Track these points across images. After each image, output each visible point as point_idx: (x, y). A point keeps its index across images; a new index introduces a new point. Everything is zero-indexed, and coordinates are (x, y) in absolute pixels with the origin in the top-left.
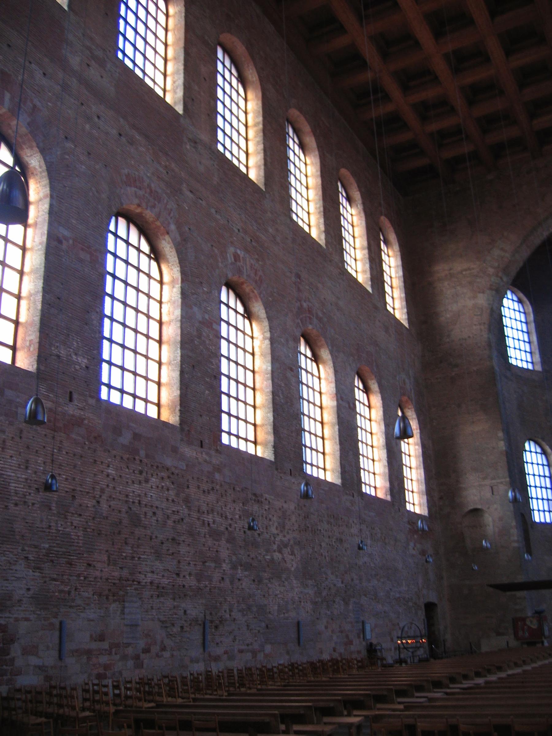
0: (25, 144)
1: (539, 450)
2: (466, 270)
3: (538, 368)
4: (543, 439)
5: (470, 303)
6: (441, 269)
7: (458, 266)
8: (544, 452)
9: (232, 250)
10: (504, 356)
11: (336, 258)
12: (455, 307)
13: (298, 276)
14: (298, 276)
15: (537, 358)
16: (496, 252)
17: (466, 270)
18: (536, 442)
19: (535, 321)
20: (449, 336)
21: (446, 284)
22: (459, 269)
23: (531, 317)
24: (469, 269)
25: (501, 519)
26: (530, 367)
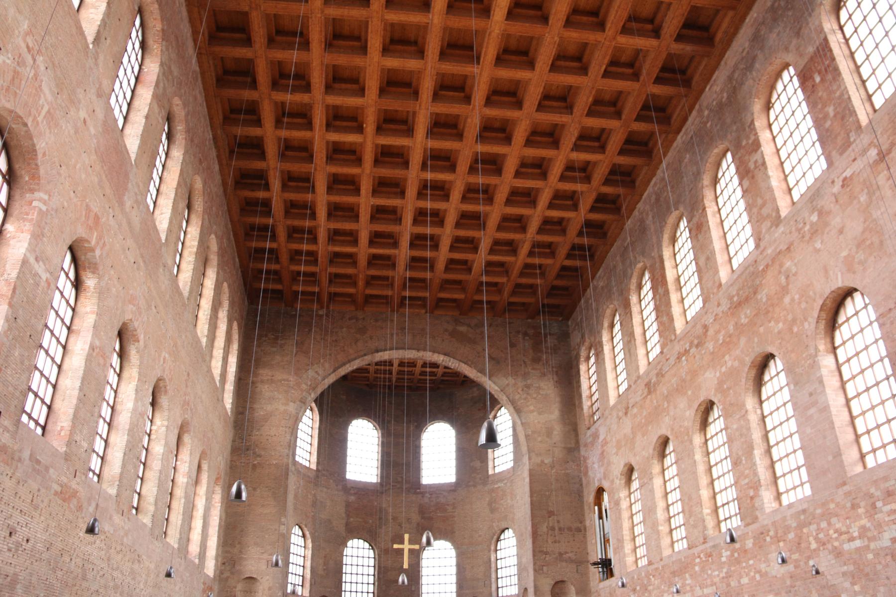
0: (89, 268)
1: (301, 534)
2: (284, 380)
3: (314, 467)
4: (306, 526)
5: (282, 408)
6: (265, 373)
7: (279, 375)
8: (304, 536)
9: (164, 354)
10: (294, 454)
11: (208, 358)
12: (269, 408)
13: (188, 374)
14: (188, 374)
15: (314, 458)
16: (311, 373)
17: (284, 380)
18: (300, 527)
19: (319, 428)
20: (259, 430)
21: (266, 386)
22: (280, 378)
23: (317, 425)
24: (288, 380)
25: (270, 589)
26: (307, 464)
